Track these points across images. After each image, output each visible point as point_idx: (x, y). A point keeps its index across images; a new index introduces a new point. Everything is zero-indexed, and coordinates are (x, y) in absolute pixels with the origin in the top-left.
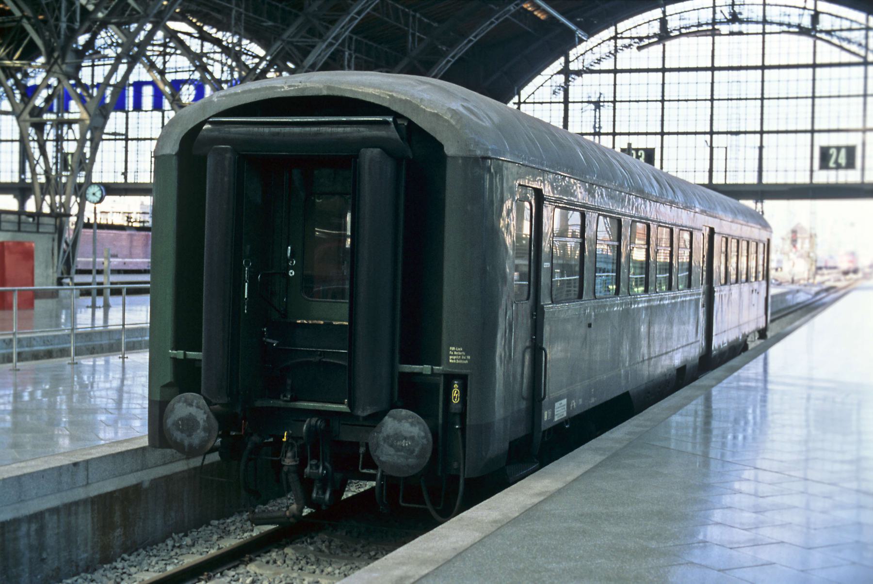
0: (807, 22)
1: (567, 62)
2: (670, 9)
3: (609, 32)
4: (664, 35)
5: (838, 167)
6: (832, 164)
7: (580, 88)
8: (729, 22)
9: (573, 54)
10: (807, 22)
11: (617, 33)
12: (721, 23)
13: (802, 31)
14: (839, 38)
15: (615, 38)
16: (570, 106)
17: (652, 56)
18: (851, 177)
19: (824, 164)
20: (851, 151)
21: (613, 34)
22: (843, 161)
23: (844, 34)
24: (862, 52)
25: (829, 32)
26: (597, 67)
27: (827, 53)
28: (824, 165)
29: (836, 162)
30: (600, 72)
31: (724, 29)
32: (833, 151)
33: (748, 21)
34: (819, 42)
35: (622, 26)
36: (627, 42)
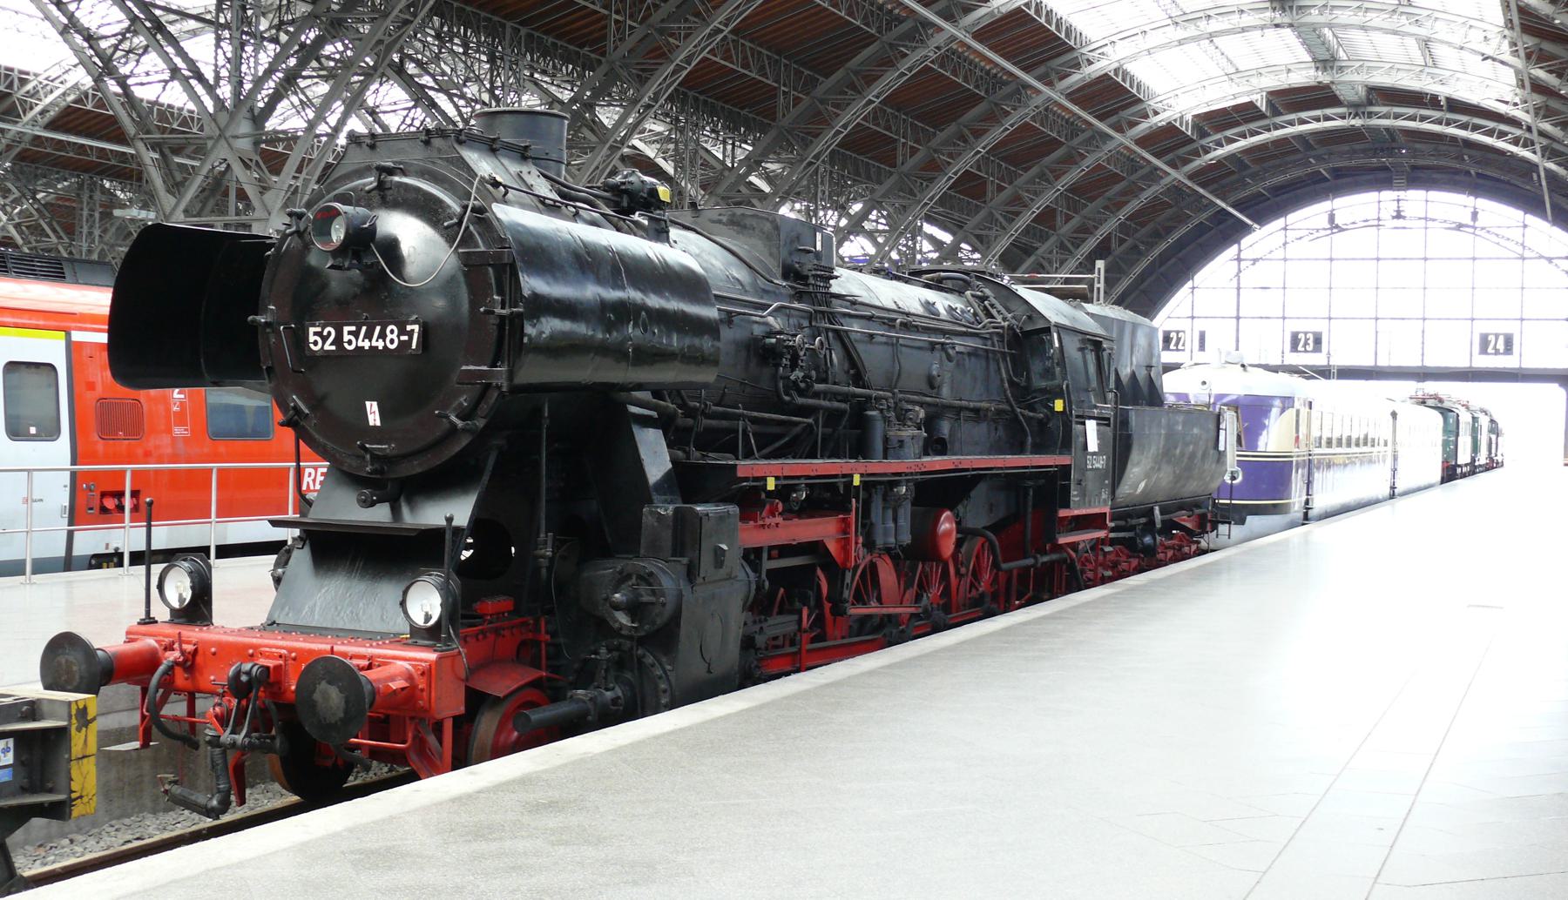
0: (1467, 220)
1: (1240, 251)
5: (1497, 352)
6: (1490, 350)
7: (1250, 276)
9: (1246, 241)
10: (1467, 220)
13: (1460, 227)
14: (1497, 235)
15: (1285, 229)
17: (1322, 247)
19: (1484, 350)
22: (1501, 346)
24: (1519, 249)
26: (1269, 256)
27: (1484, 247)
28: (1484, 350)
29: (1495, 348)
32: (1492, 338)
36: (1299, 234)
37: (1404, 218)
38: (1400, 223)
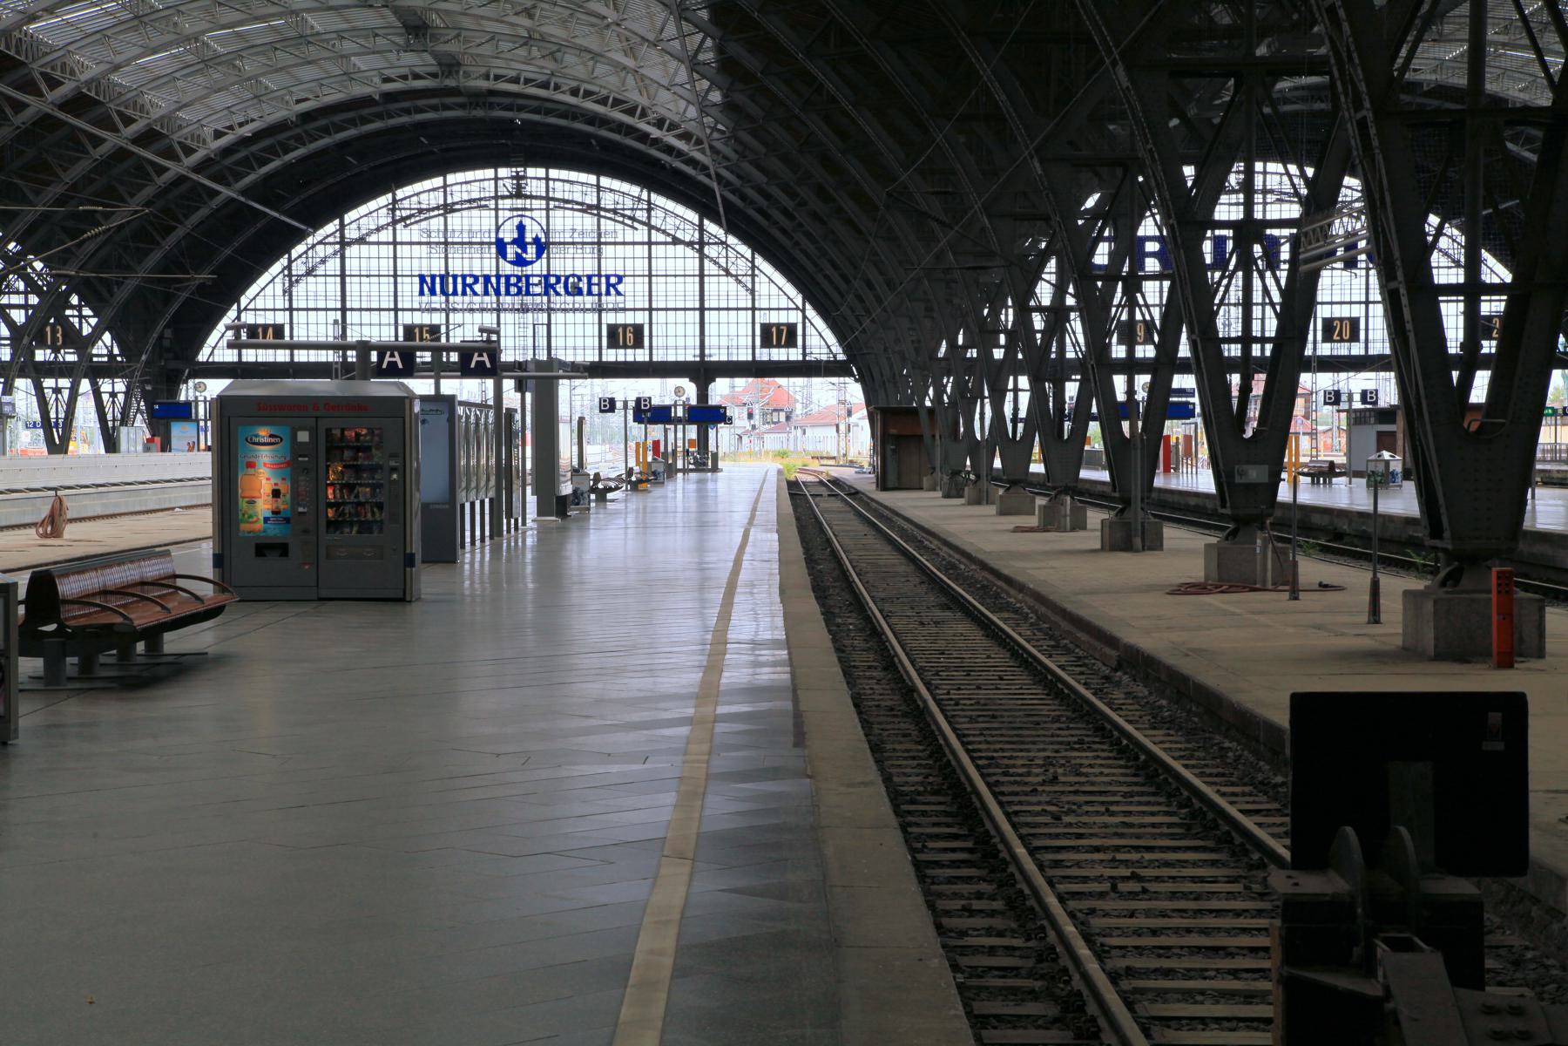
2: (451, 178)
3: (385, 199)
4: (448, 209)
8: (511, 196)
11: (395, 201)
12: (503, 197)
13: (587, 209)
16: (348, 279)
18: (641, 355)
20: (638, 330)
21: (390, 201)
22: (630, 342)
23: (628, 213)
25: (615, 211)
30: (378, 243)
31: (508, 203)
33: (531, 197)
34: (602, 220)
35: (400, 194)
36: (405, 213)
37: (526, 197)
38: (519, 203)
